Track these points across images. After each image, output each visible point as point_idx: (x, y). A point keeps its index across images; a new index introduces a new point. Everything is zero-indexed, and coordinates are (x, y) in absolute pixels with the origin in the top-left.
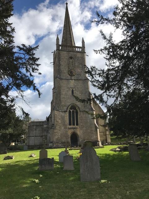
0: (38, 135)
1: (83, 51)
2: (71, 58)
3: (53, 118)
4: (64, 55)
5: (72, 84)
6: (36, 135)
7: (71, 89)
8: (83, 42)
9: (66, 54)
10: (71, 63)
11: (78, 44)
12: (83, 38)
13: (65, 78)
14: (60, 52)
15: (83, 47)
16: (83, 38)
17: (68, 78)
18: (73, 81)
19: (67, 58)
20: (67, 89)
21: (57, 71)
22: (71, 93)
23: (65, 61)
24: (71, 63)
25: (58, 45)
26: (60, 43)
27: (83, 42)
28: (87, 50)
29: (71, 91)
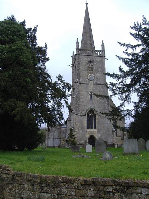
0: (56, 137)
1: (102, 55)
2: (90, 62)
3: (72, 121)
4: (84, 60)
5: (91, 89)
6: (55, 137)
7: (90, 94)
8: (103, 45)
9: (86, 58)
10: (90, 67)
11: (98, 47)
12: (103, 41)
13: (83, 83)
14: (80, 56)
15: (103, 51)
16: (103, 41)
17: (86, 83)
18: (92, 85)
19: (86, 62)
20: (86, 94)
21: (77, 75)
22: (90, 97)
23: (84, 65)
24: (90, 67)
25: (77, 49)
26: (80, 48)
27: (103, 45)
28: (106, 54)
29: (90, 95)
